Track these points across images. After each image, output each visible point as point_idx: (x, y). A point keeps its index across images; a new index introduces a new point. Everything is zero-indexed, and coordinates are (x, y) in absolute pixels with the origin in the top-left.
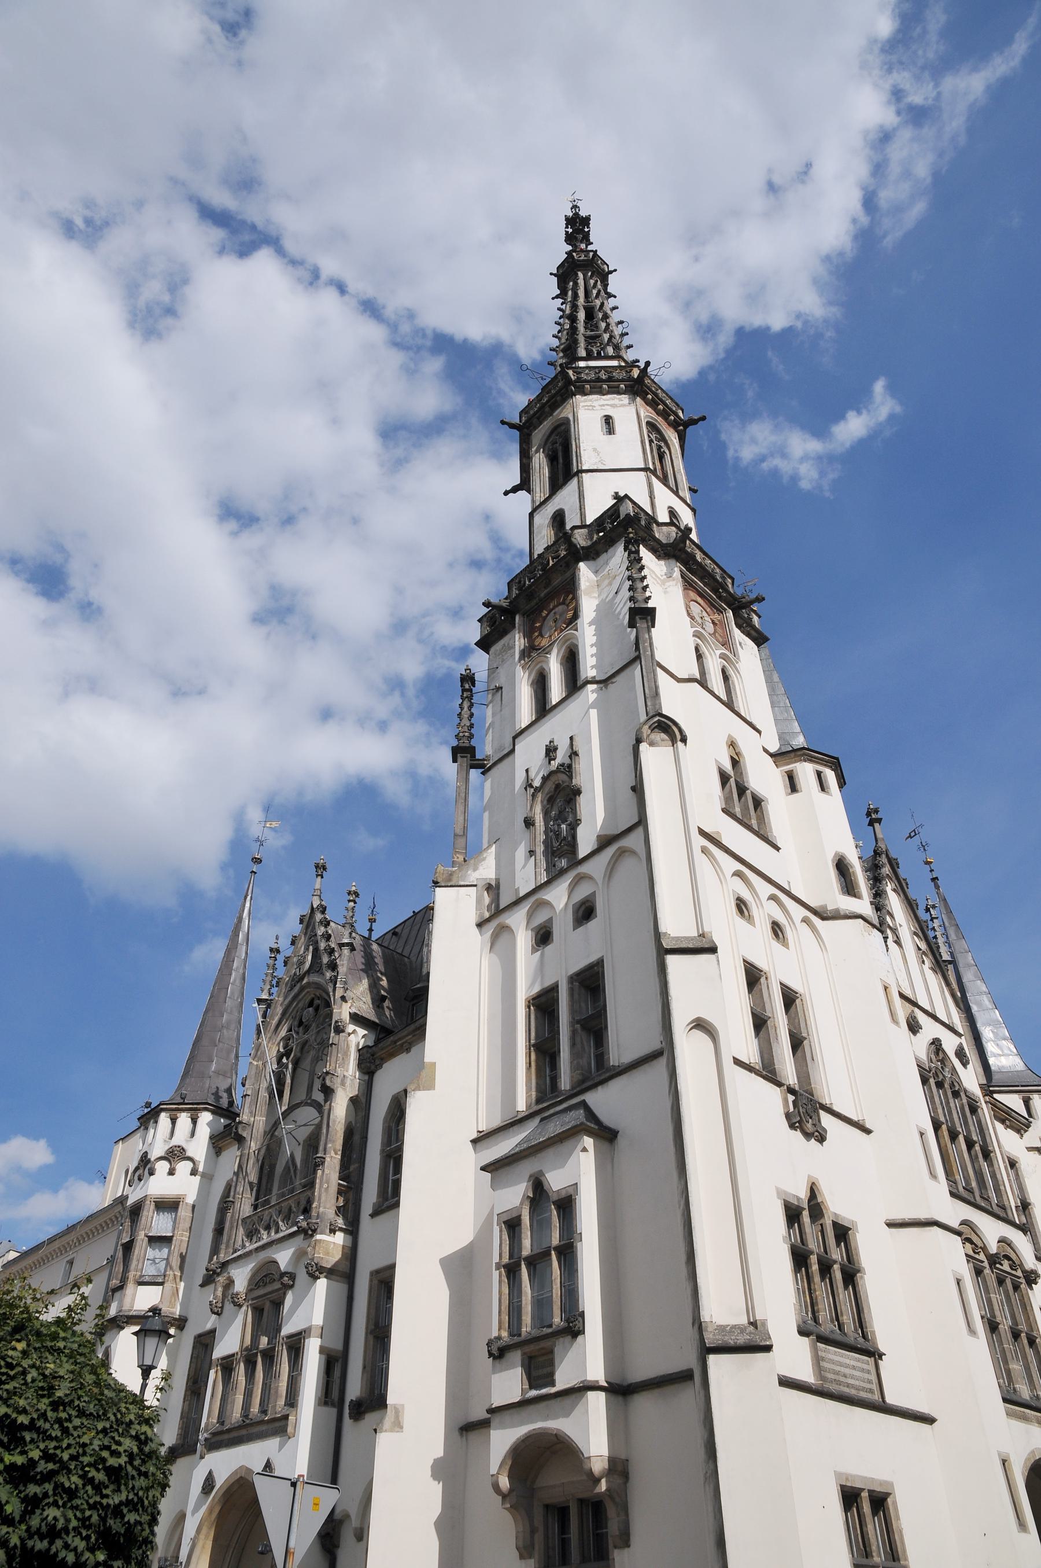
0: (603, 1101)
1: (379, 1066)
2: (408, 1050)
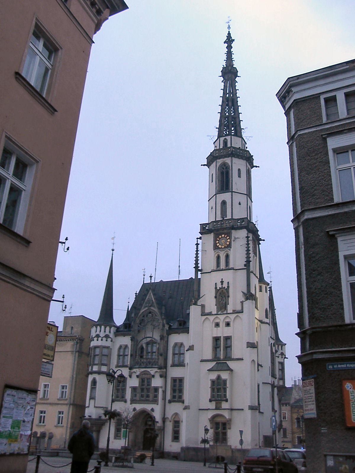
0: (231, 364)
1: (170, 334)
2: (179, 334)
